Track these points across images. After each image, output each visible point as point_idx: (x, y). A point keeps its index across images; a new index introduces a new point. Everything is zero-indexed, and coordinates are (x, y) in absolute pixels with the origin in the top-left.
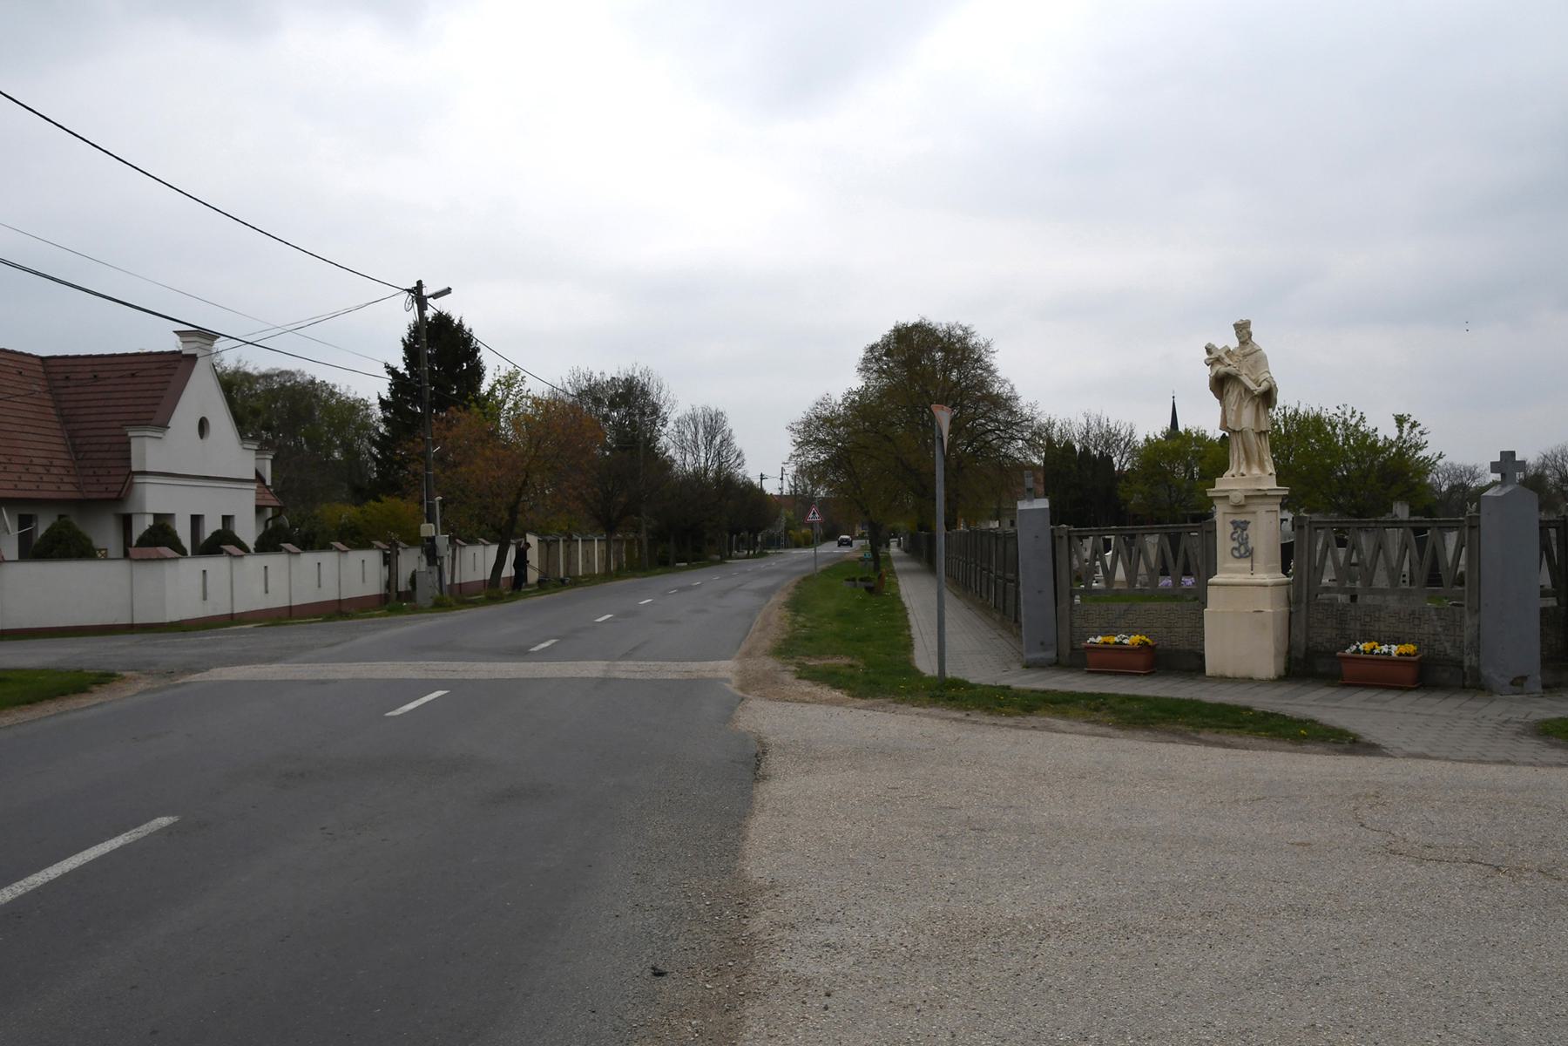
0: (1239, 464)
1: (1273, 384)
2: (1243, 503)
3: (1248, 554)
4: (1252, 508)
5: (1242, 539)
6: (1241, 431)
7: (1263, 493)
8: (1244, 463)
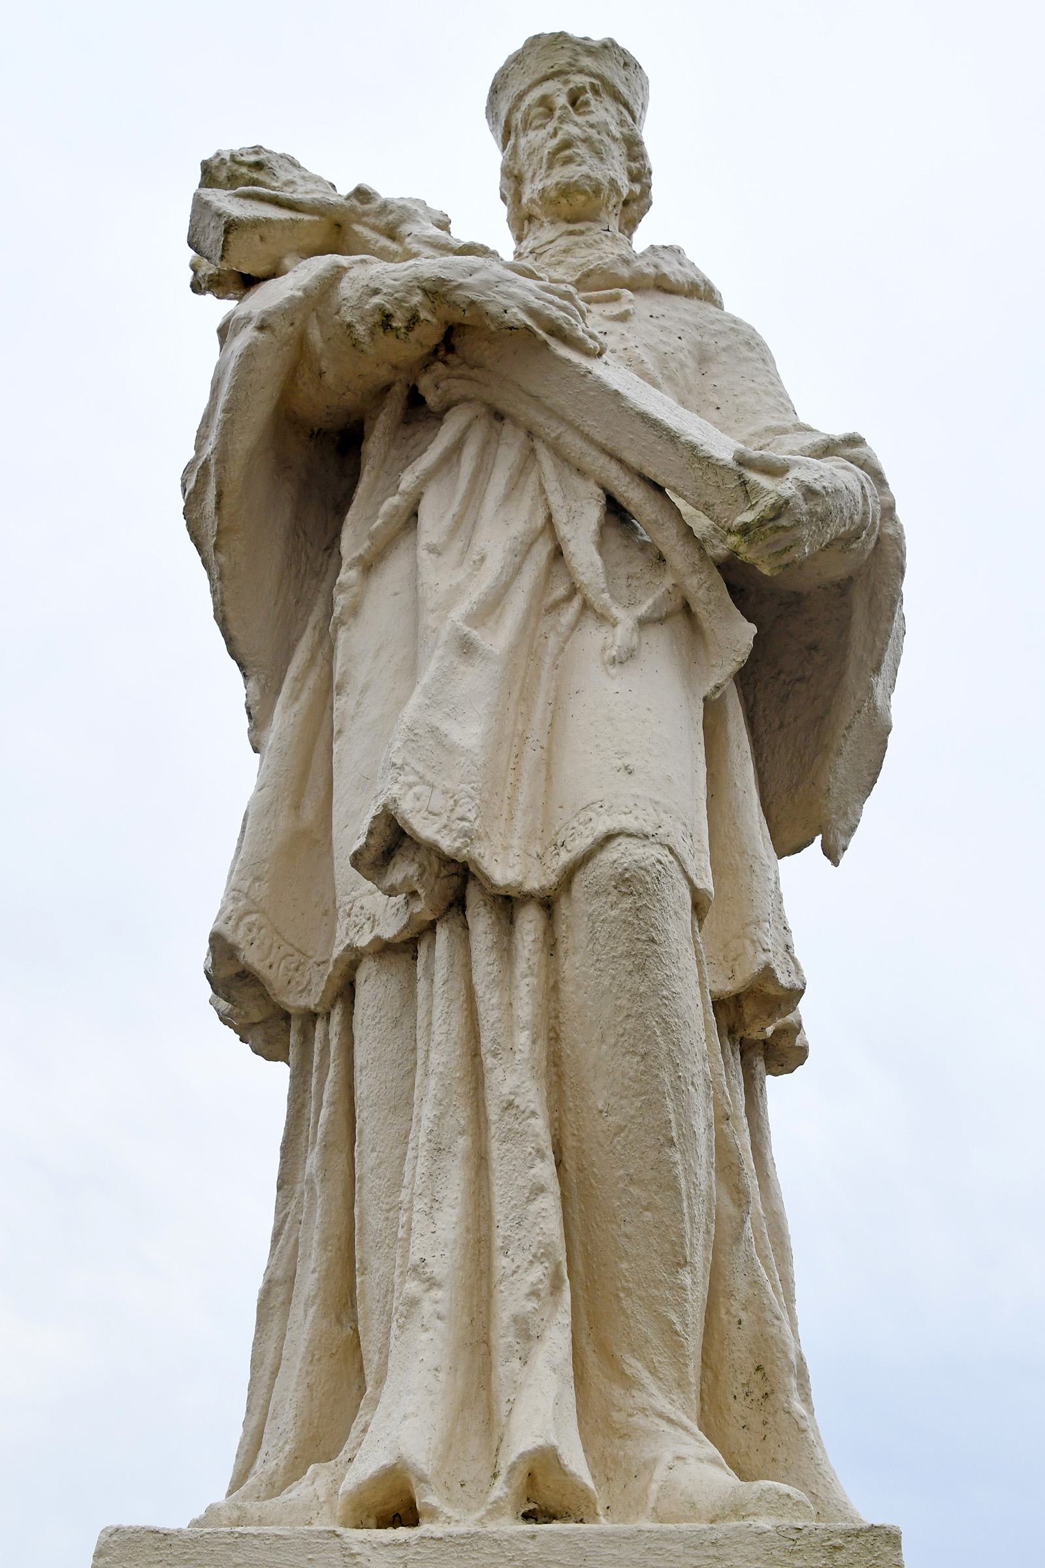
6: (548, 904)
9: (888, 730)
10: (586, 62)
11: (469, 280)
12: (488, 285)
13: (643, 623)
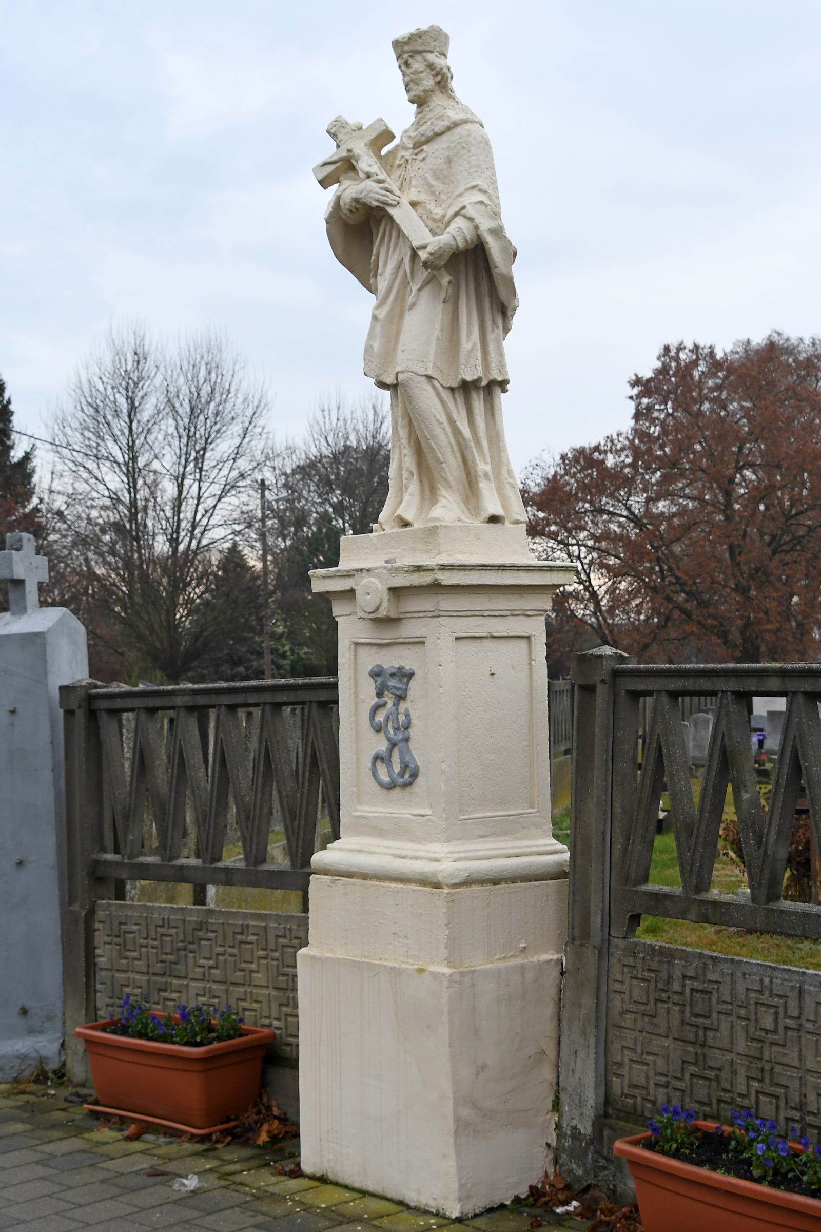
0: (401, 490)
1: (485, 225)
2: (383, 613)
3: (407, 776)
4: (410, 629)
5: (396, 729)
7: (425, 579)
8: (414, 487)
9: (512, 278)
10: (406, 48)
11: (362, 196)
12: (366, 196)
13: (420, 290)
